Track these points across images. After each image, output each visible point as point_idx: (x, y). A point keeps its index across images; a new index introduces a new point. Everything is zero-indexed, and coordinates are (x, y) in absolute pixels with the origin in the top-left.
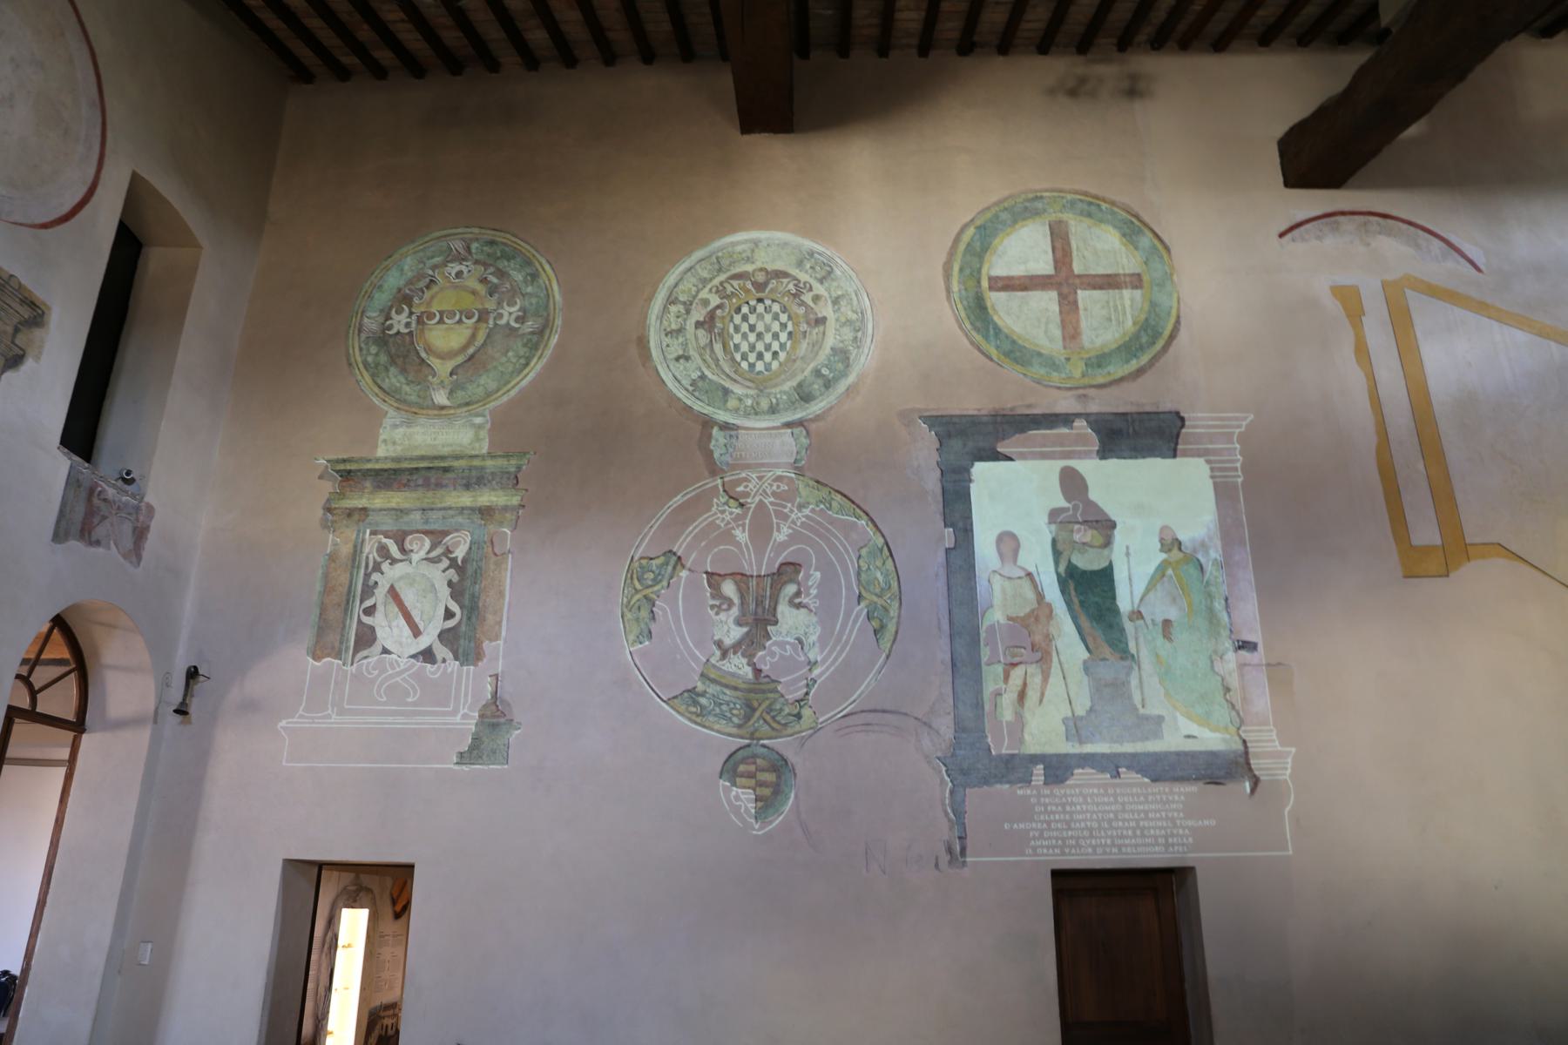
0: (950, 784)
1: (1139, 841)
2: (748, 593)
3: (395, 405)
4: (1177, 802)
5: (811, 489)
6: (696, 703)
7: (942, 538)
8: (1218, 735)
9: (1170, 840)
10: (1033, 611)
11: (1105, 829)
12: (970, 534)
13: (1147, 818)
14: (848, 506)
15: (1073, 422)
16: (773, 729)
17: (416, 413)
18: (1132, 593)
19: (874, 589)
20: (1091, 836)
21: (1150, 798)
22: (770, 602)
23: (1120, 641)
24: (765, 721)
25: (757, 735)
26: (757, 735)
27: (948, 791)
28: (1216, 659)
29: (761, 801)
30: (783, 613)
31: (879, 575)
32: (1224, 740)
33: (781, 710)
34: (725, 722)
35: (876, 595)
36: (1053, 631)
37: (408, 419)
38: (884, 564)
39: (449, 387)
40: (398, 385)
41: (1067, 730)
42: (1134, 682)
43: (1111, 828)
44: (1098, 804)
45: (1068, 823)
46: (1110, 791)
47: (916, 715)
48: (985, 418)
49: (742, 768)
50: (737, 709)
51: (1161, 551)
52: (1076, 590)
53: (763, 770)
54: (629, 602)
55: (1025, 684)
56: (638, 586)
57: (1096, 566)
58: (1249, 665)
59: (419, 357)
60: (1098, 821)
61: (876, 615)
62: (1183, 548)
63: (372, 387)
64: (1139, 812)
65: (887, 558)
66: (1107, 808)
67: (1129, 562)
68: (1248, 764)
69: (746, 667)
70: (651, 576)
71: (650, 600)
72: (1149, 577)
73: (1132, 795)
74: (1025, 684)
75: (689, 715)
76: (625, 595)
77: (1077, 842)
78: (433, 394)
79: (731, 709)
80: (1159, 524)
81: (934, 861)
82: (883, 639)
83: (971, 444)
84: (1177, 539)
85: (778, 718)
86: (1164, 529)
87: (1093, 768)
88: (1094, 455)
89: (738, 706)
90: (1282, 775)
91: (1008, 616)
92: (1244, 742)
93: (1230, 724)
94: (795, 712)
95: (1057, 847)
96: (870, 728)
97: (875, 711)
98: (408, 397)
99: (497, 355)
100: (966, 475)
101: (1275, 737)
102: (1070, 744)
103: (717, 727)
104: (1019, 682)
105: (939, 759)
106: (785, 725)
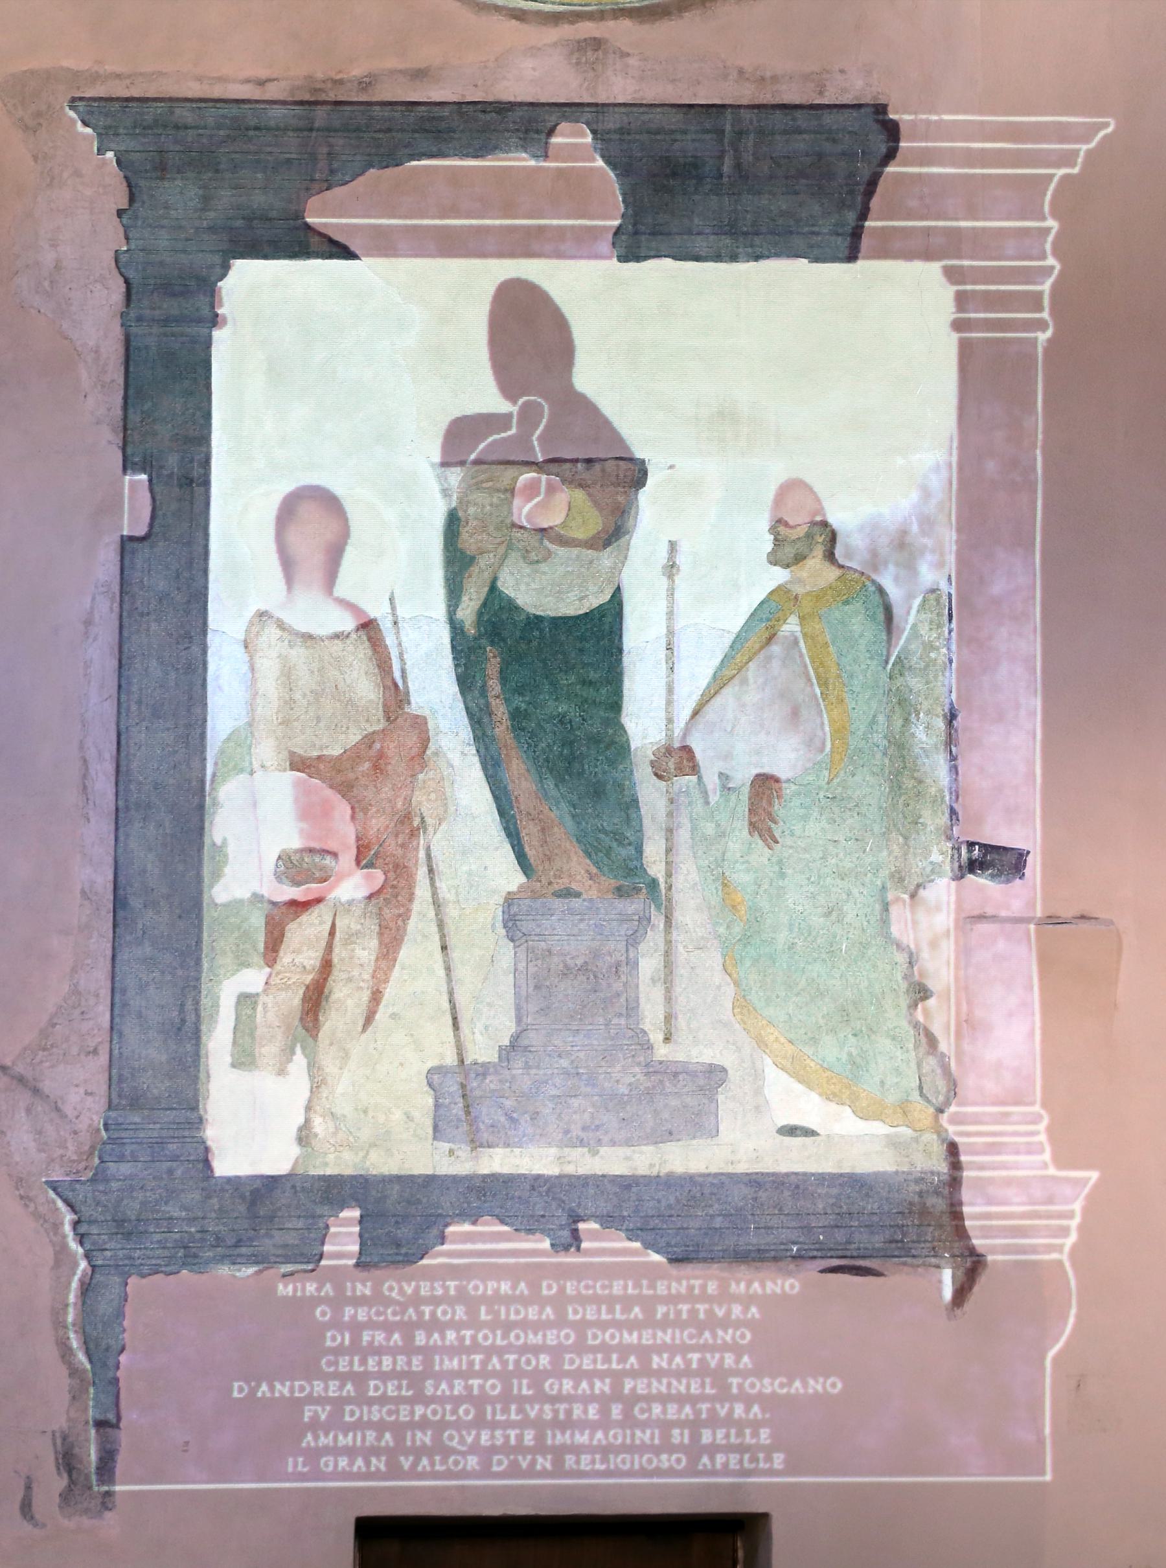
0: (83, 1264)
1: (616, 1436)
4: (738, 1324)
7: (111, 506)
8: (878, 1128)
9: (706, 1437)
10: (369, 740)
11: (521, 1400)
12: (199, 490)
13: (646, 1371)
15: (551, 132)
18: (670, 690)
20: (480, 1422)
21: (661, 1310)
23: (620, 839)
27: (75, 1284)
28: (898, 899)
32: (893, 1143)
36: (425, 804)
41: (437, 1106)
42: (649, 964)
43: (542, 1397)
44: (508, 1327)
45: (415, 1380)
46: (549, 1289)
48: (277, 112)
51: (774, 559)
52: (504, 679)
55: (327, 966)
57: (571, 606)
58: (994, 918)
60: (505, 1376)
62: (839, 552)
64: (625, 1351)
66: (534, 1339)
67: (671, 592)
68: (957, 1215)
72: (728, 640)
73: (611, 1301)
74: (327, 966)
77: (437, 1438)
80: (778, 472)
81: (20, 1495)
83: (225, 197)
84: (825, 524)
86: (791, 488)
87: (503, 1222)
88: (605, 246)
90: (1050, 1248)
91: (292, 754)
92: (953, 1149)
93: (915, 1096)
95: (375, 1451)
100: (202, 301)
101: (1043, 1138)
102: (447, 1146)
104: (311, 958)
105: (54, 1186)
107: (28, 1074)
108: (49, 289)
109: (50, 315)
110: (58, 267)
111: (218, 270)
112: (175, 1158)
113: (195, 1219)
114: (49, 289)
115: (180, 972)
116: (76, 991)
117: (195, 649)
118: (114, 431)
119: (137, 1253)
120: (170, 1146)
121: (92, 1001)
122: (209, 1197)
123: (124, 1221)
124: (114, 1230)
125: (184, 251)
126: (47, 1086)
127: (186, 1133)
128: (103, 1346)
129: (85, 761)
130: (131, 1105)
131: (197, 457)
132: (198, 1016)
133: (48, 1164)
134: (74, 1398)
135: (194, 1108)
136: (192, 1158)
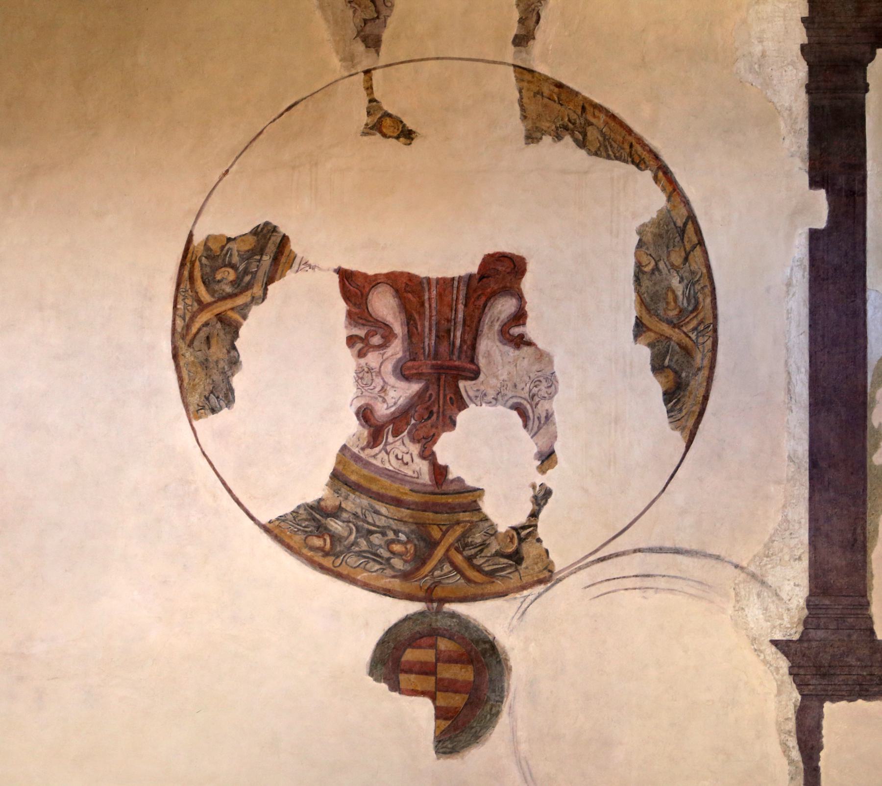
2: (422, 314)
5: (546, 100)
6: (321, 530)
12: (859, 199)
14: (620, 138)
16: (469, 580)
19: (666, 310)
22: (463, 334)
24: (455, 567)
25: (439, 592)
26: (439, 592)
29: (446, 719)
30: (488, 355)
31: (675, 282)
33: (484, 545)
34: (377, 567)
35: (670, 322)
38: (686, 259)
47: (735, 560)
49: (410, 655)
50: (399, 542)
53: (451, 660)
54: (188, 327)
56: (206, 297)
61: (667, 362)
65: (694, 247)
69: (417, 460)
70: (231, 275)
71: (230, 325)
75: (310, 554)
76: (180, 312)
79: (389, 543)
82: (681, 410)
85: (478, 561)
89: (403, 537)
94: (510, 550)
96: (648, 582)
97: (660, 550)
103: (362, 576)
106: (492, 574)
107: (758, 572)
108: (757, 70)
109: (759, 87)
110: (763, 55)
111: (868, 56)
112: (852, 628)
113: (866, 667)
114: (757, 70)
115: (853, 509)
116: (786, 520)
117: (858, 301)
118: (802, 161)
119: (830, 688)
120: (849, 620)
121: (797, 526)
122: (875, 653)
123: (820, 667)
124: (814, 673)
125: (846, 44)
126: (770, 580)
127: (859, 612)
128: (810, 746)
129: (789, 373)
130: (824, 593)
131: (857, 178)
132: (865, 537)
133: (772, 630)
134: (792, 778)
135: (864, 596)
136: (862, 628)
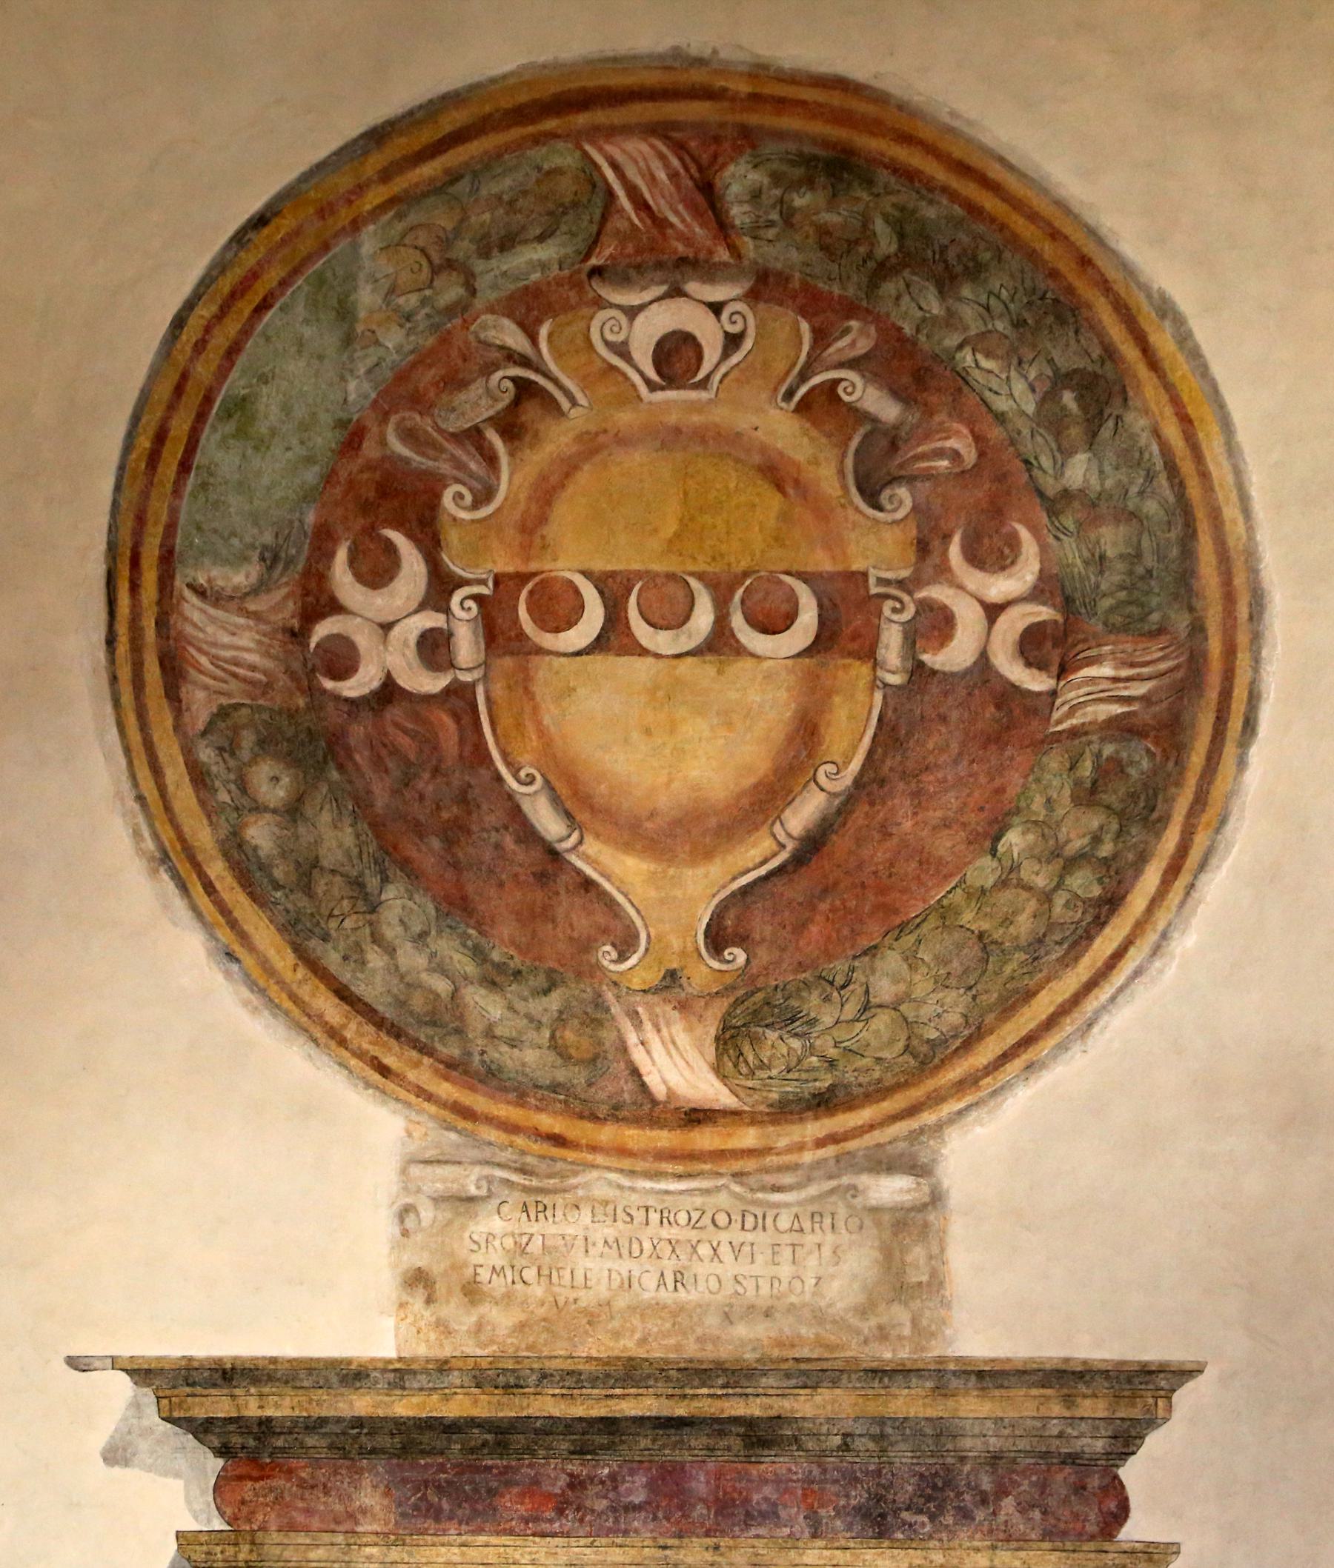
3: (446, 1090)
17: (558, 1140)
37: (523, 1171)
39: (720, 1007)
40: (442, 986)
59: (528, 834)
63: (304, 992)
78: (632, 1038)
98: (504, 1056)
99: (944, 845)
